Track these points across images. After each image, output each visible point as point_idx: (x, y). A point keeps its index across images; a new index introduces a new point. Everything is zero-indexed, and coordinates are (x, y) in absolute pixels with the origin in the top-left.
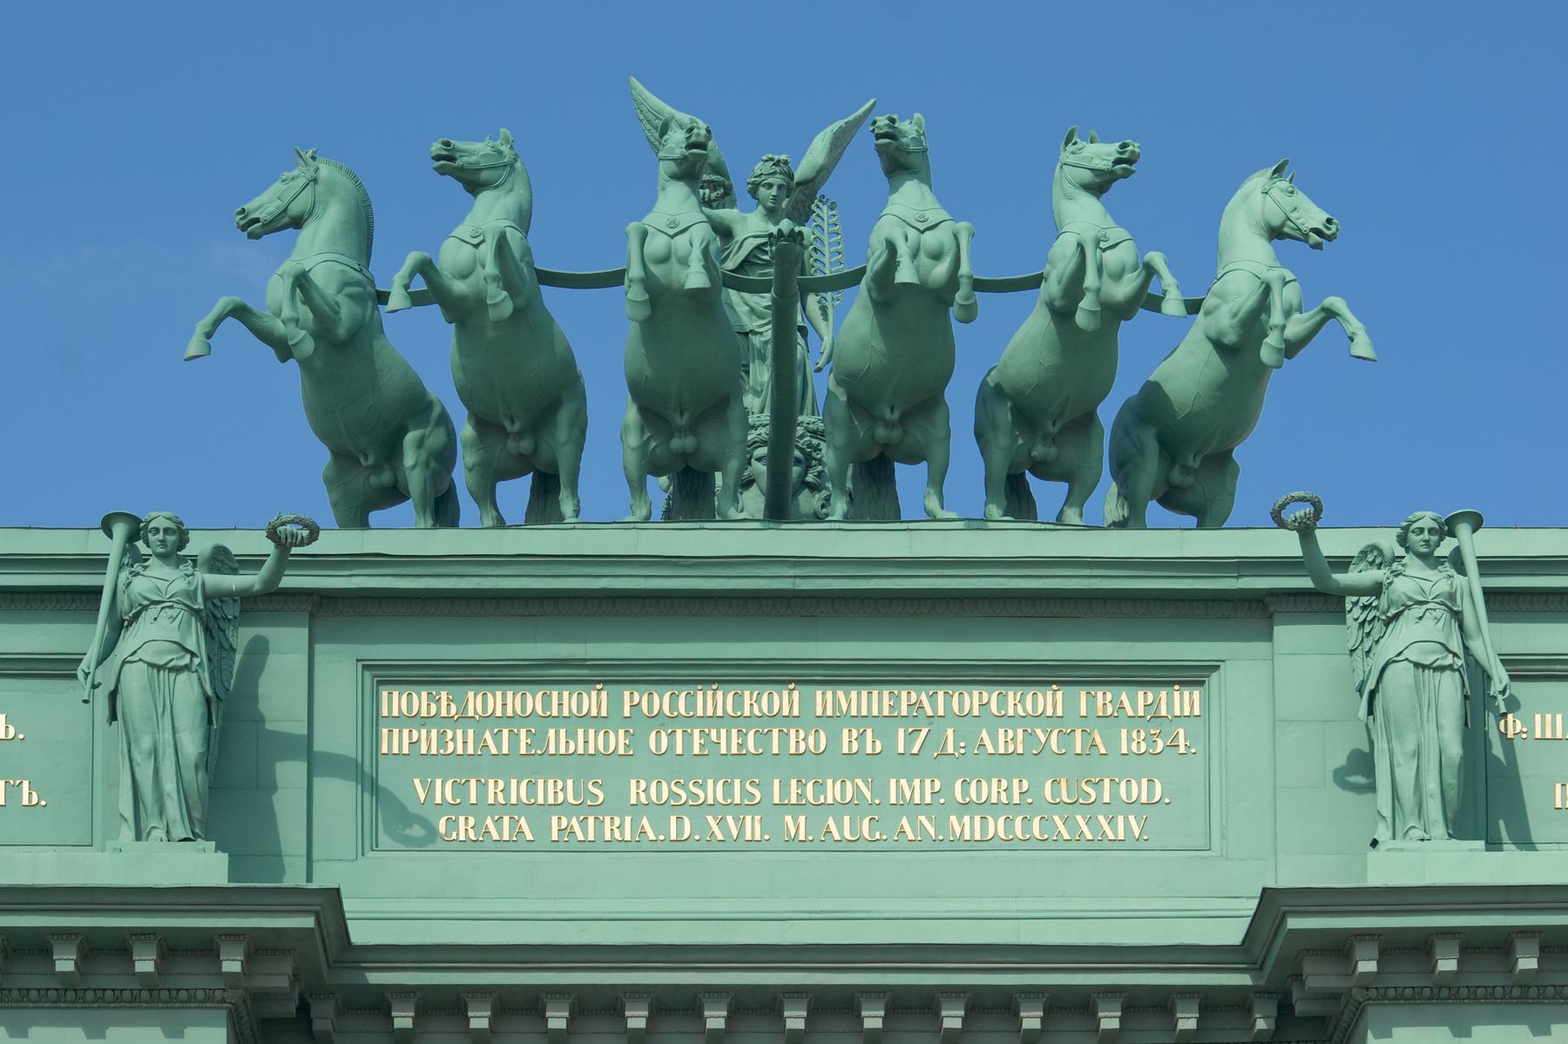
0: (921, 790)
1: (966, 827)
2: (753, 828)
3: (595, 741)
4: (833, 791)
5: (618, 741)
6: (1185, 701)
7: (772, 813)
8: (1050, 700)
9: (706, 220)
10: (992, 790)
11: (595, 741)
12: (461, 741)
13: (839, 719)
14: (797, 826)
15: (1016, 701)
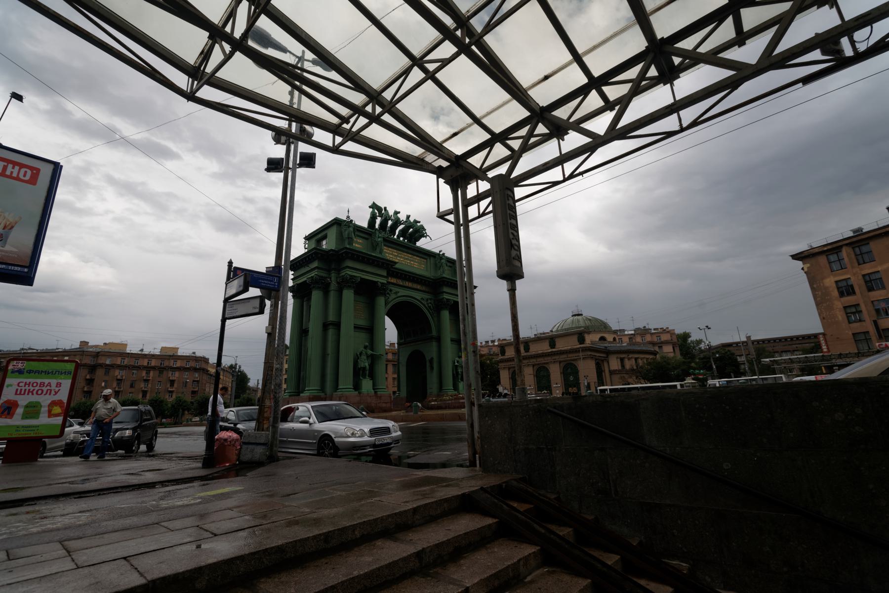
0: (413, 263)
1: (415, 266)
2: (404, 263)
3: (395, 254)
4: (408, 261)
5: (397, 254)
6: (425, 261)
7: (405, 262)
8: (419, 258)
9: (513, 249)
10: (416, 264)
11: (395, 254)
12: (388, 251)
13: (408, 256)
14: (406, 263)
15: (417, 258)
